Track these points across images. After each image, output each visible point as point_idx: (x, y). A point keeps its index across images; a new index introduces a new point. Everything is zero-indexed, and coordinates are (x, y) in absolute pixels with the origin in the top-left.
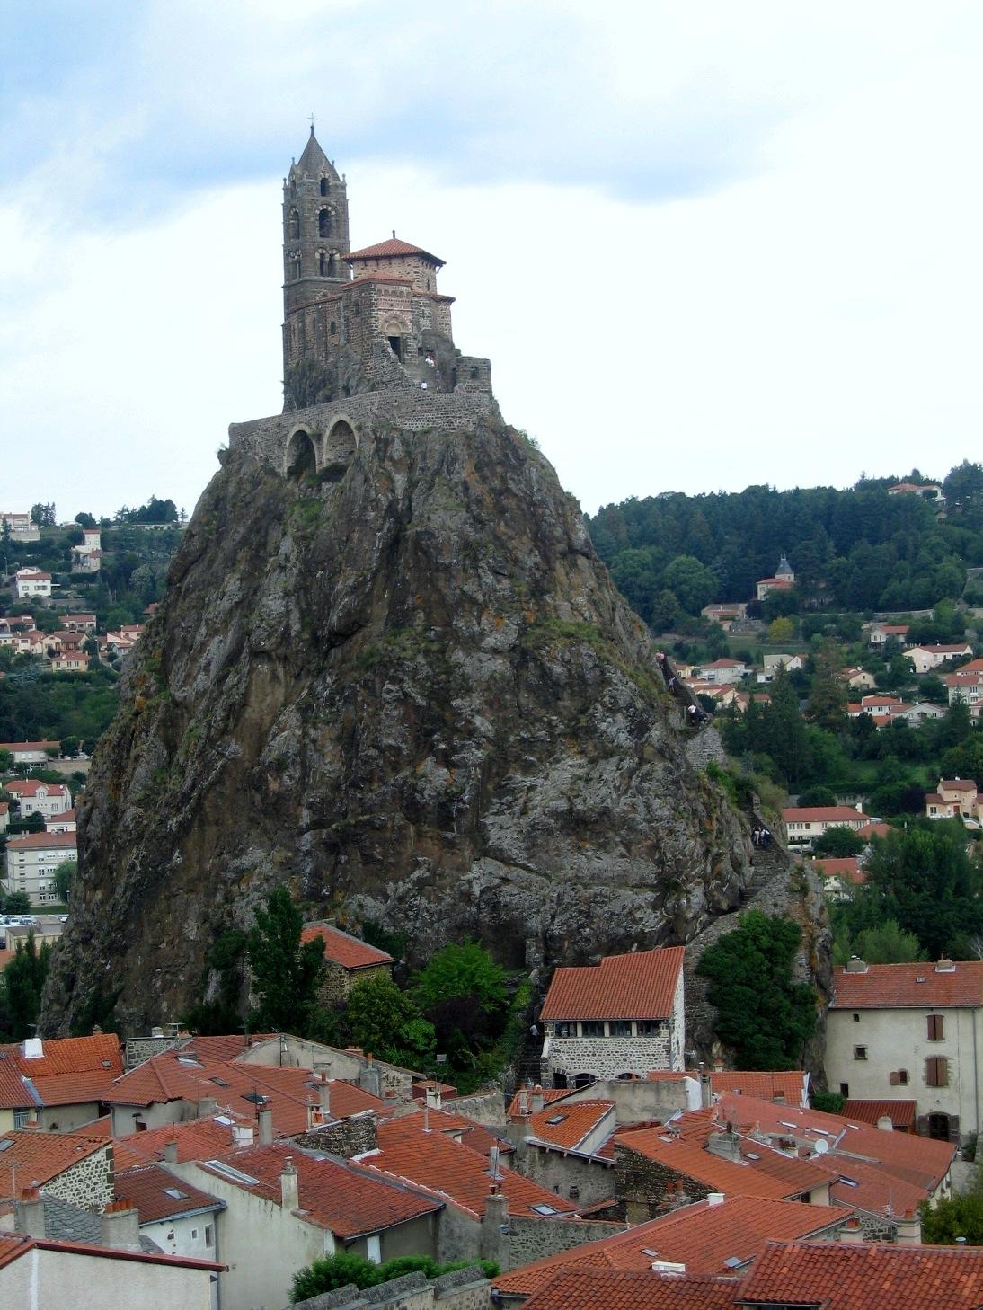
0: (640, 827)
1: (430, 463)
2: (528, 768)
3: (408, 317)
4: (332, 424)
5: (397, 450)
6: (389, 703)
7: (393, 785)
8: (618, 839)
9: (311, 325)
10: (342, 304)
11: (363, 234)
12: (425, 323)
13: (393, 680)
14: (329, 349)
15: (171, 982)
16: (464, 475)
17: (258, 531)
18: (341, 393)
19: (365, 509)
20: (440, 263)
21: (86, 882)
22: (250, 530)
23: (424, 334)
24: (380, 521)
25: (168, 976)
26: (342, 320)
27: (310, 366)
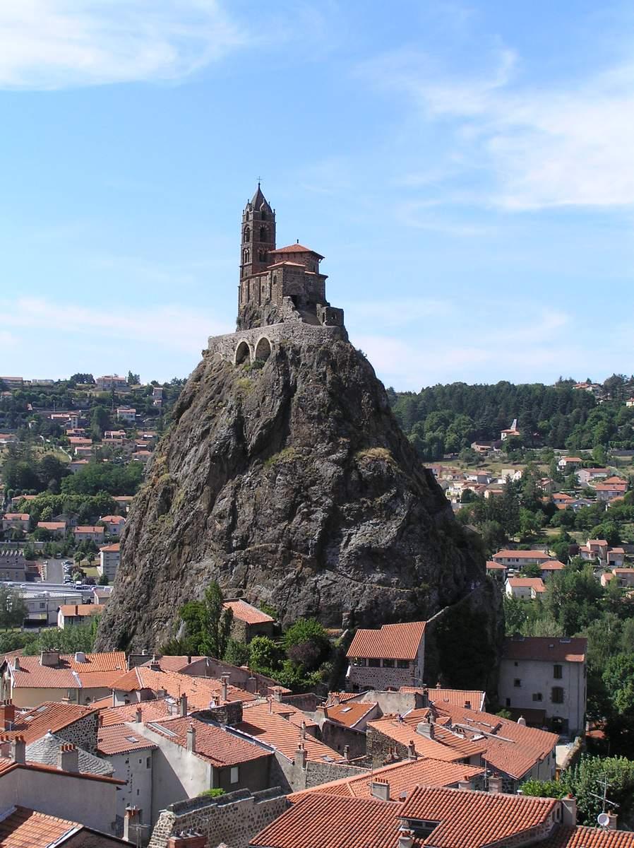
0: (406, 558)
2: (349, 525)
3: (302, 285)
4: (259, 339)
5: (289, 354)
7: (279, 529)
8: (394, 563)
11: (283, 241)
12: (311, 289)
15: (162, 626)
17: (219, 393)
20: (322, 258)
21: (123, 571)
23: (310, 294)
25: (161, 623)
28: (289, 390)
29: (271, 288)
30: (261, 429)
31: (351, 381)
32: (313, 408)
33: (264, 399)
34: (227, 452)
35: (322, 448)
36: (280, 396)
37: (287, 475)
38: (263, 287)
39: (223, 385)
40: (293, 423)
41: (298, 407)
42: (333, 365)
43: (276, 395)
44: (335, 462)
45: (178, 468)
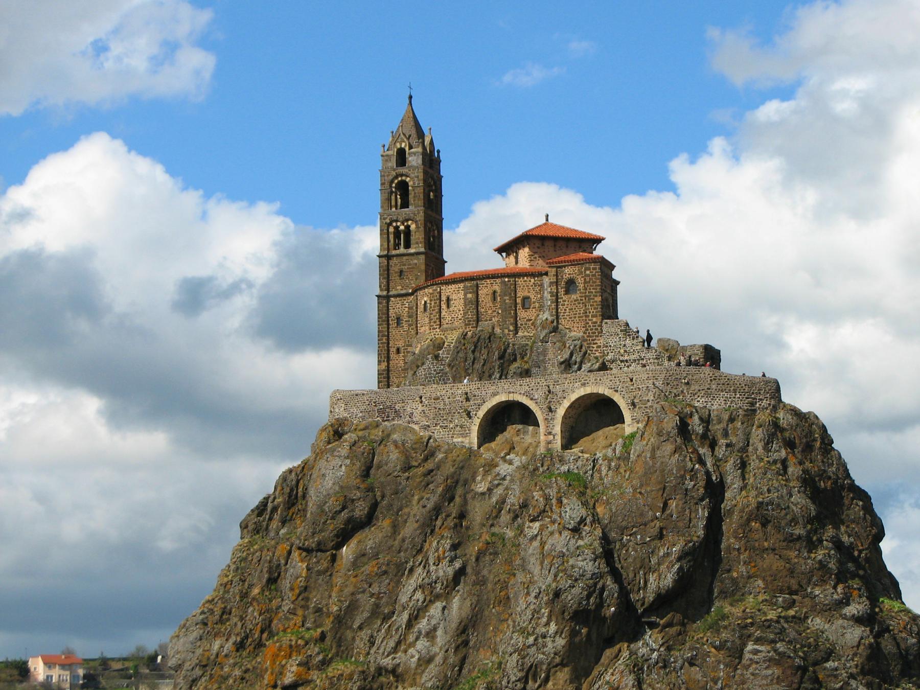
1: (734, 440)
5: (695, 424)
6: (757, 663)
9: (490, 297)
10: (546, 280)
13: (758, 641)
14: (519, 323)
16: (783, 453)
17: (452, 499)
18: (554, 370)
19: (683, 477)
22: (442, 496)
24: (702, 491)
26: (547, 295)
27: (489, 338)
28: (715, 490)
29: (557, 302)
30: (679, 559)
31: (830, 478)
32: (794, 521)
33: (666, 505)
34: (600, 605)
35: (824, 593)
36: (702, 500)
37: (773, 642)
38: (525, 299)
39: (457, 482)
40: (739, 549)
41: (749, 521)
42: (790, 444)
43: (693, 497)
44: (858, 620)
45: (399, 643)
